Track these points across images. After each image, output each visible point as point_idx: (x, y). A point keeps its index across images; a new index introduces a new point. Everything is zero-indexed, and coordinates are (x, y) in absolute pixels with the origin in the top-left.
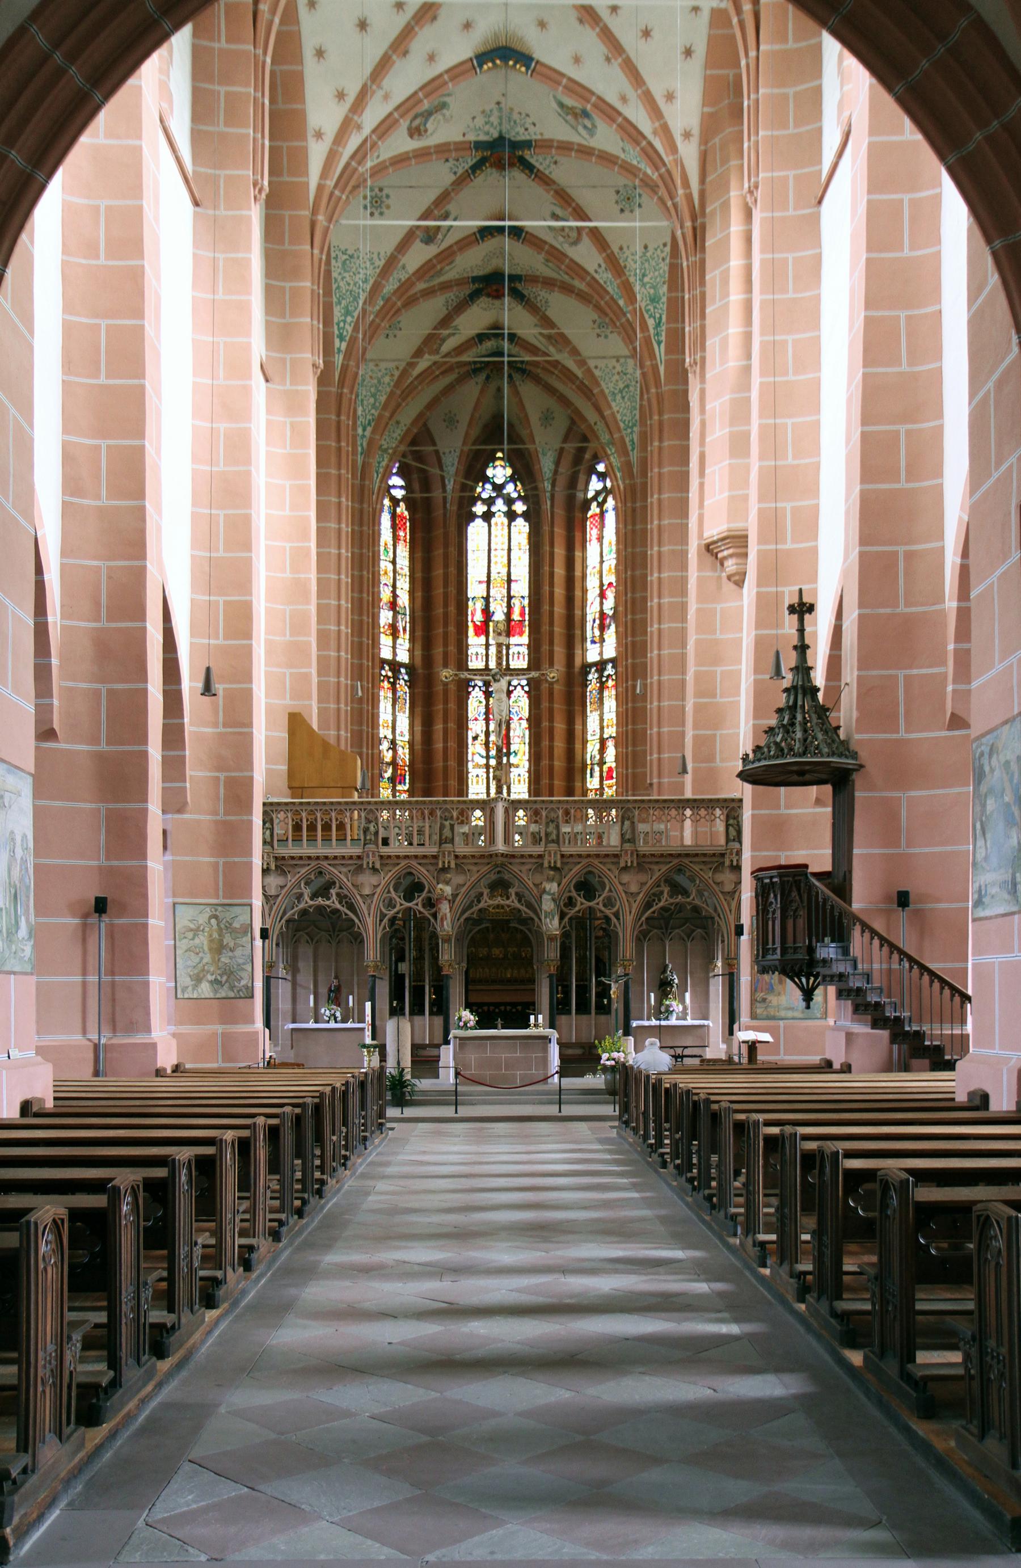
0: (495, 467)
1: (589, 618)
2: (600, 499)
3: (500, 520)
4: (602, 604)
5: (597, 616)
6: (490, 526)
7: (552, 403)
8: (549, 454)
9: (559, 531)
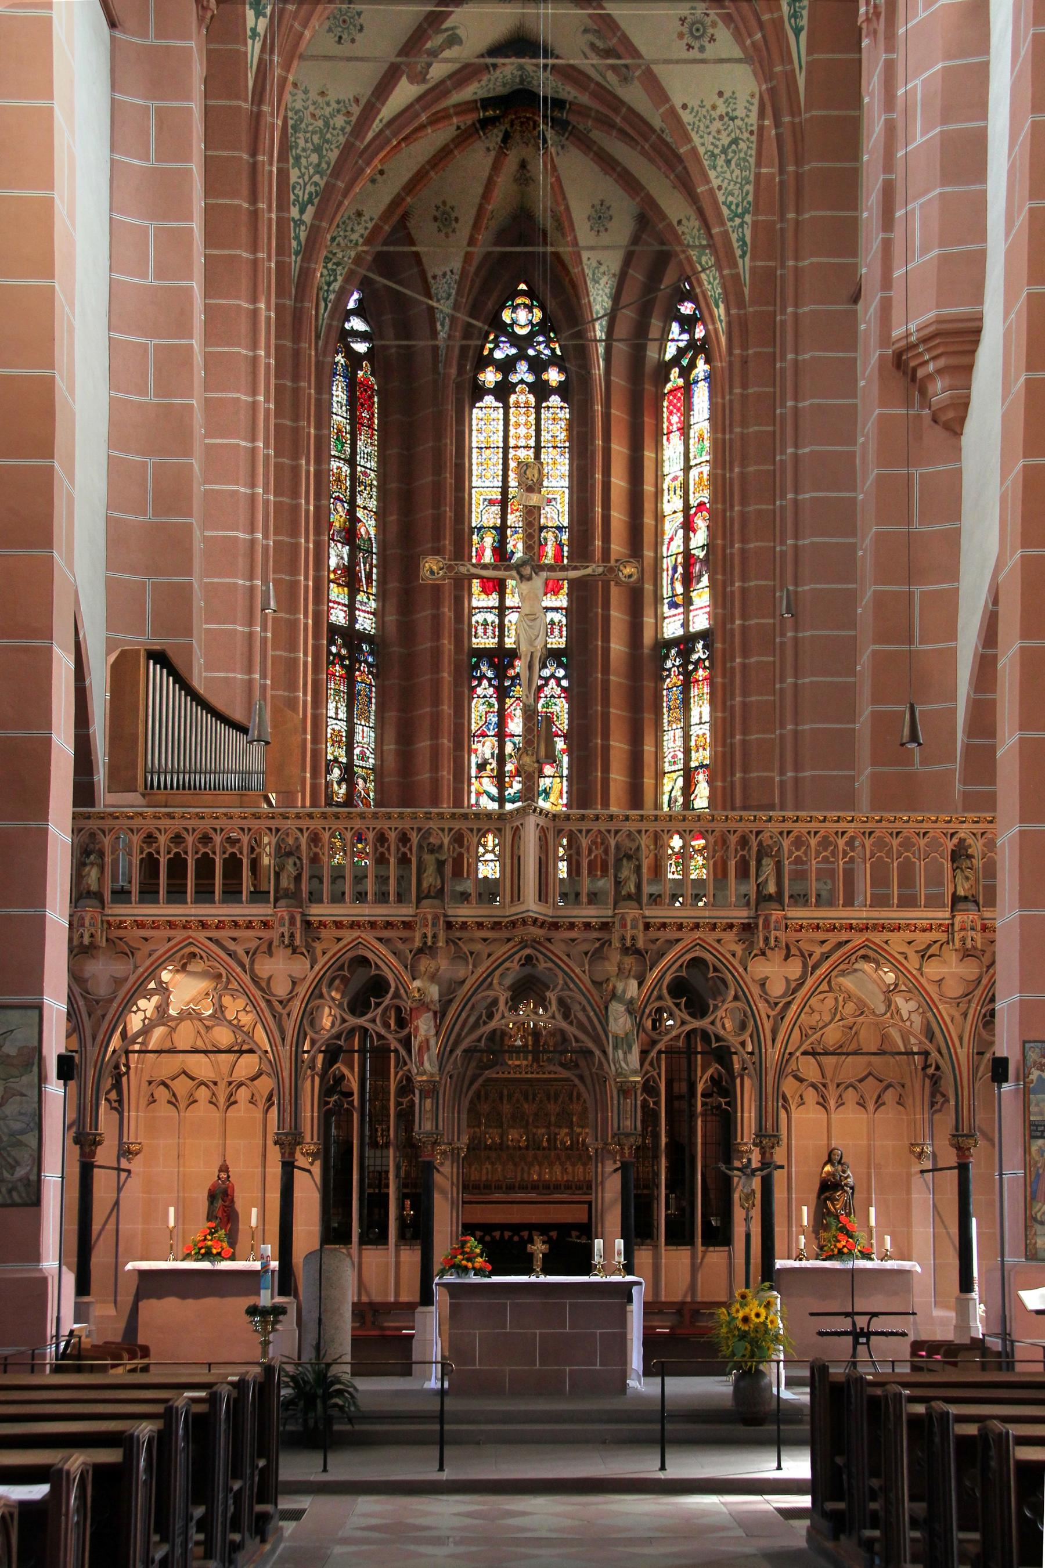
0: (515, 308)
1: (668, 563)
2: (685, 362)
3: (522, 397)
4: (687, 540)
5: (680, 559)
6: (506, 408)
7: (608, 188)
8: (603, 282)
9: (619, 414)
